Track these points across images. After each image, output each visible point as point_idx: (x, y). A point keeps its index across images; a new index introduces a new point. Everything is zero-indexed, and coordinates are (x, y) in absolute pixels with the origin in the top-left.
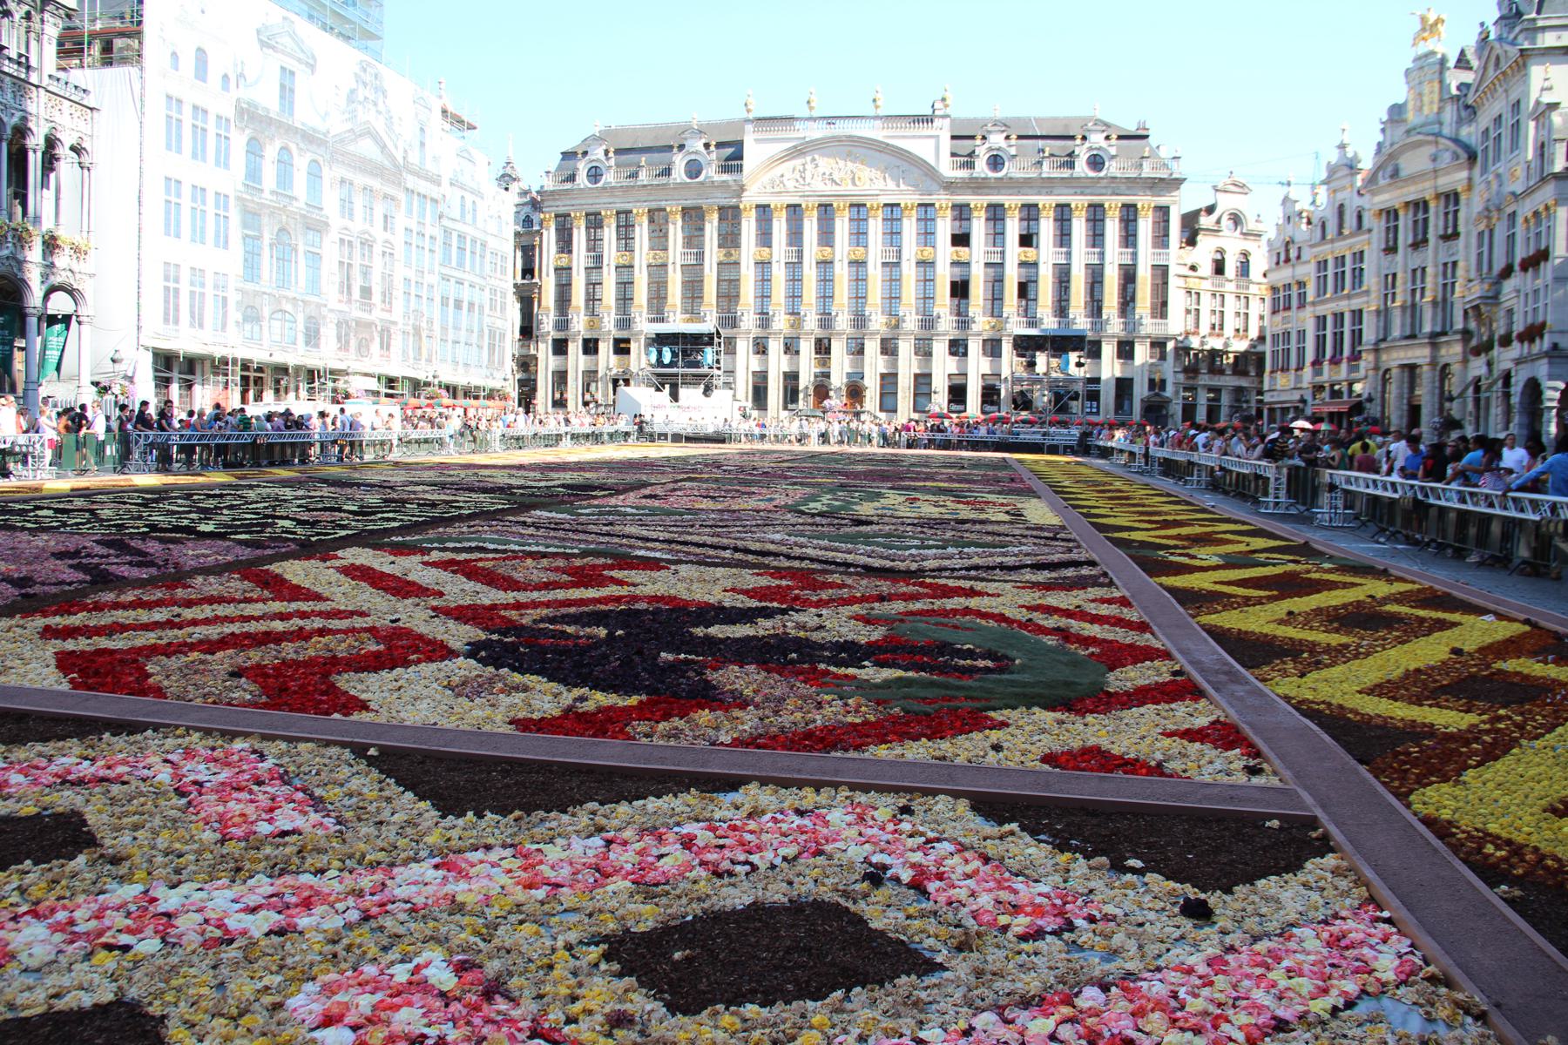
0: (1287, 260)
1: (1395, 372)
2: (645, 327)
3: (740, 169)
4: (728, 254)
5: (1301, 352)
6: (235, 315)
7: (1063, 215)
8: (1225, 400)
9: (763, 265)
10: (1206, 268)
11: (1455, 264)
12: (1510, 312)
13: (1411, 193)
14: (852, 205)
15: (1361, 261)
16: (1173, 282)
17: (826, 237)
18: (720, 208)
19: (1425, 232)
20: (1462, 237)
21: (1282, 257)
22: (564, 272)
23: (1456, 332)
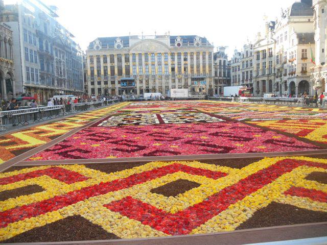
0: (235, 62)
1: (260, 82)
2: (117, 79)
3: (129, 46)
5: (239, 79)
6: (39, 78)
10: (218, 64)
12: (286, 70)
16: (213, 66)
17: (147, 60)
19: (265, 56)
22: (92, 68)
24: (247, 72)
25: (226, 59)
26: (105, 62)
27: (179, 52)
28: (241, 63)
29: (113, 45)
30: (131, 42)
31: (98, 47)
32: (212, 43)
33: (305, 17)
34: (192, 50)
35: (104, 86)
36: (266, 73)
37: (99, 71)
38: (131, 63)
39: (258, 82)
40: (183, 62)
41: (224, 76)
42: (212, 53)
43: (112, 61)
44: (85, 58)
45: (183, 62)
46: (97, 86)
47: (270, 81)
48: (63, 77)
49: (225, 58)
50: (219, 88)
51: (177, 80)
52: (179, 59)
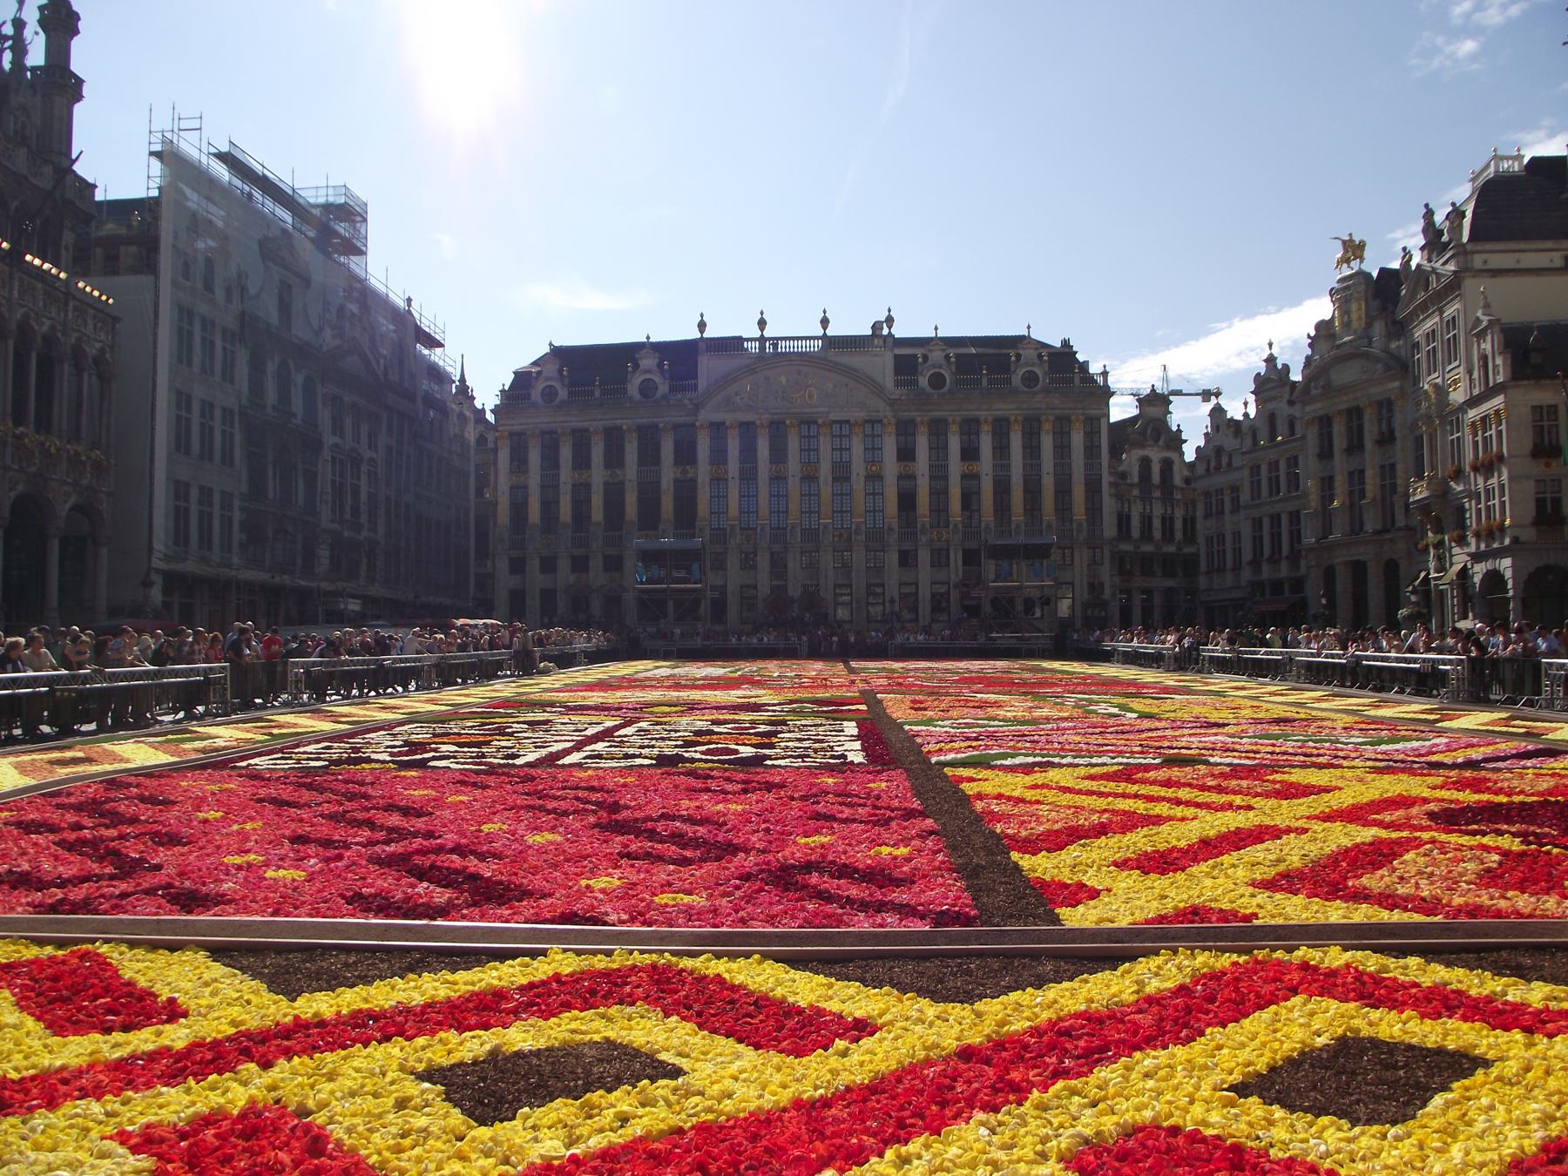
0: (1218, 468)
4: (684, 472)
5: (1238, 552)
7: (1001, 430)
8: (1157, 600)
9: (719, 480)
10: (1135, 478)
11: (1393, 466)
13: (1344, 402)
14: (802, 423)
15: (1296, 465)
16: (1106, 490)
17: (779, 454)
18: (676, 427)
20: (1398, 443)
21: (1213, 464)
23: (1400, 529)
24: (1275, 519)
25: (1173, 455)
26: (582, 461)
27: (937, 414)
28: (1246, 472)
29: (624, 381)
30: (708, 368)
31: (549, 394)
32: (1105, 374)
33: (1549, 244)
34: (1004, 408)
35: (572, 578)
36: (1369, 527)
37: (549, 507)
38: (703, 472)
39: (1329, 574)
40: (955, 466)
41: (1168, 534)
42: (1103, 421)
43: (614, 459)
44: (491, 445)
45: (955, 466)
46: (536, 579)
47: (1391, 568)
48: (365, 534)
49: (1168, 447)
50: (1138, 599)
51: (924, 556)
52: (939, 449)
